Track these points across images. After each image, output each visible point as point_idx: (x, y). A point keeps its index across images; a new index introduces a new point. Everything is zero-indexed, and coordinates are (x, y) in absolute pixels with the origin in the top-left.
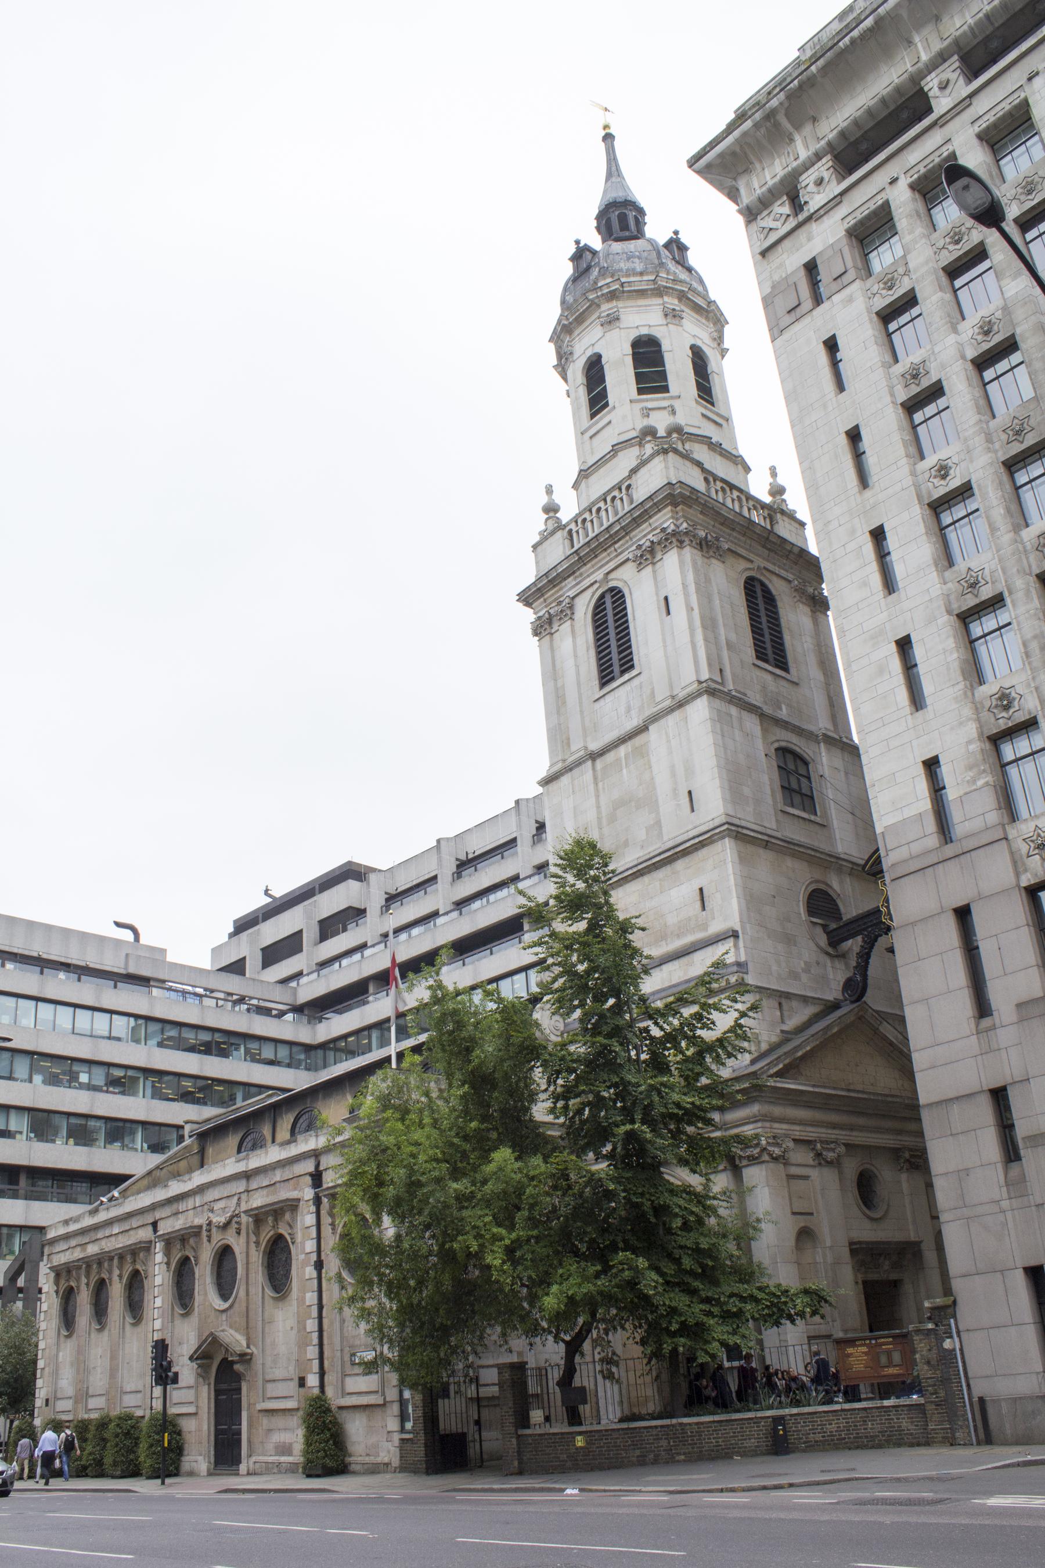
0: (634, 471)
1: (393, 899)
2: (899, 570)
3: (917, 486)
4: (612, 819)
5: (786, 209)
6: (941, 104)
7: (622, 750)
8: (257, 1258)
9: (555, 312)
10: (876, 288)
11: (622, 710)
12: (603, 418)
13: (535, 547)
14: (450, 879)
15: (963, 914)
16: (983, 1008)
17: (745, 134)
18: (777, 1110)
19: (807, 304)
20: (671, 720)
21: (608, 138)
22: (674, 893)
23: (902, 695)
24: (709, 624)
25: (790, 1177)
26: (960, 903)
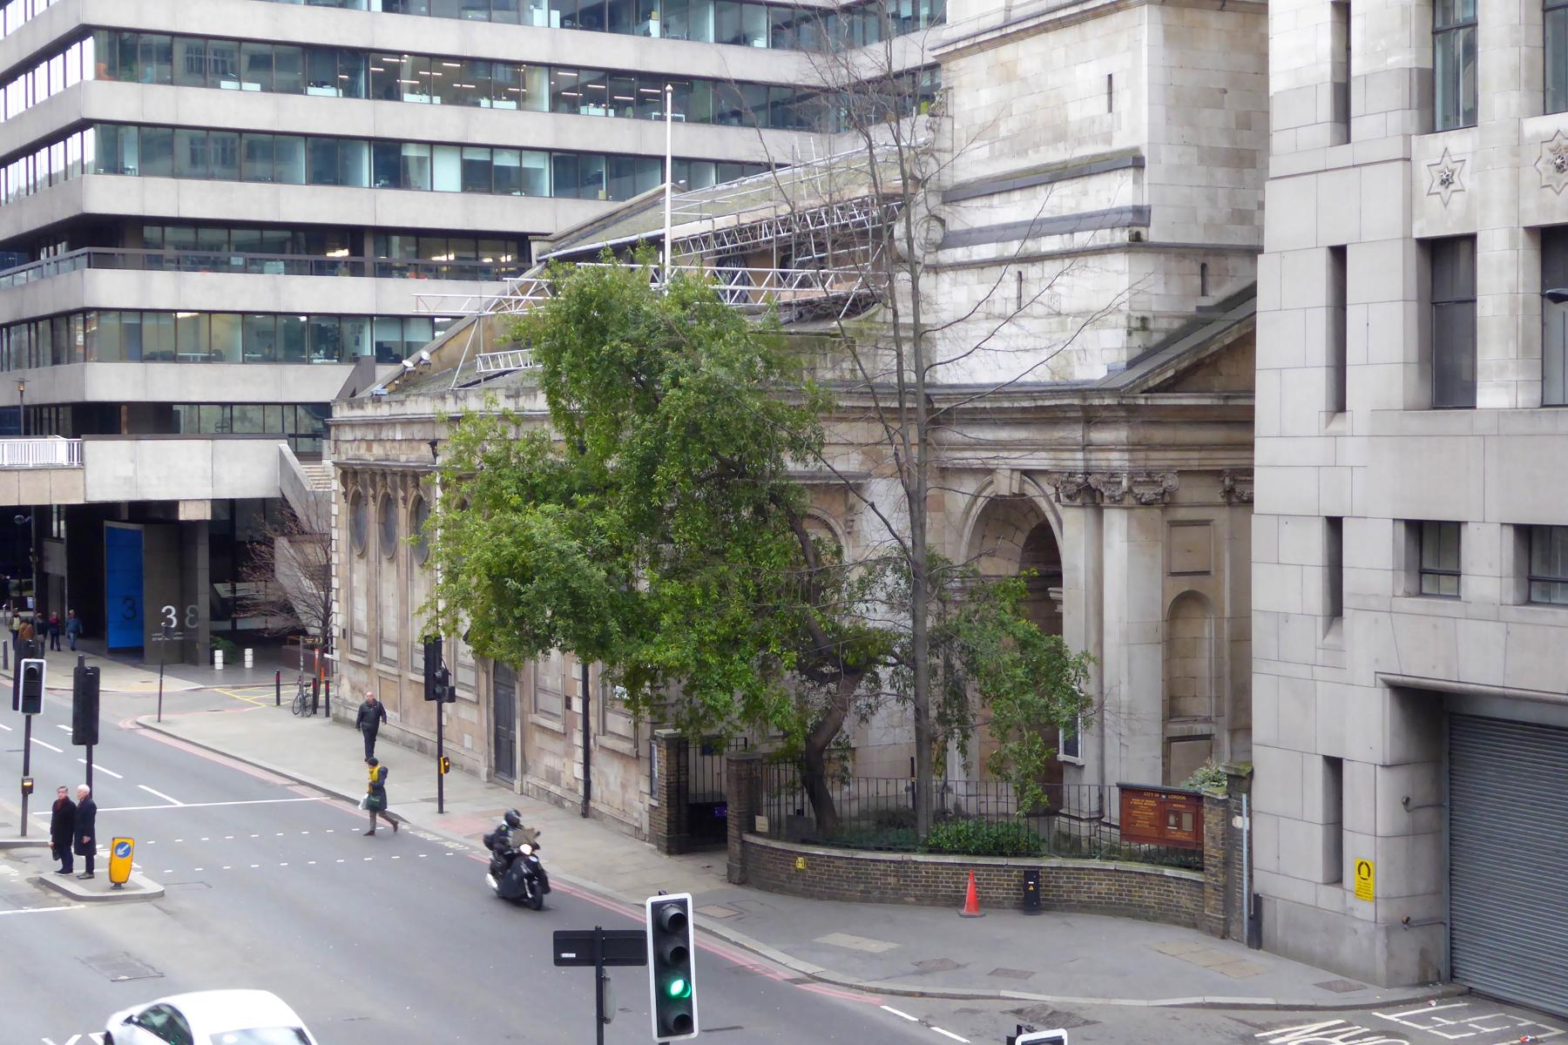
18: (1160, 435)
25: (1175, 524)
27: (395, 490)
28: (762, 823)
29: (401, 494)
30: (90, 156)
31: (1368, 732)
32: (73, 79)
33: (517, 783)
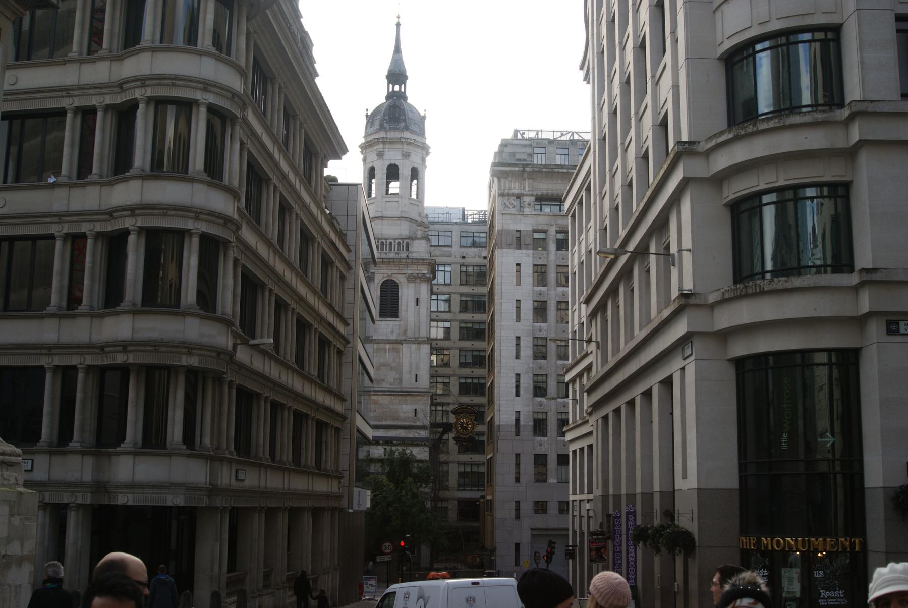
2: (522, 353)
7: (388, 346)
11: (390, 330)
16: (518, 480)
20: (414, 346)
22: (404, 406)
31: (525, 538)
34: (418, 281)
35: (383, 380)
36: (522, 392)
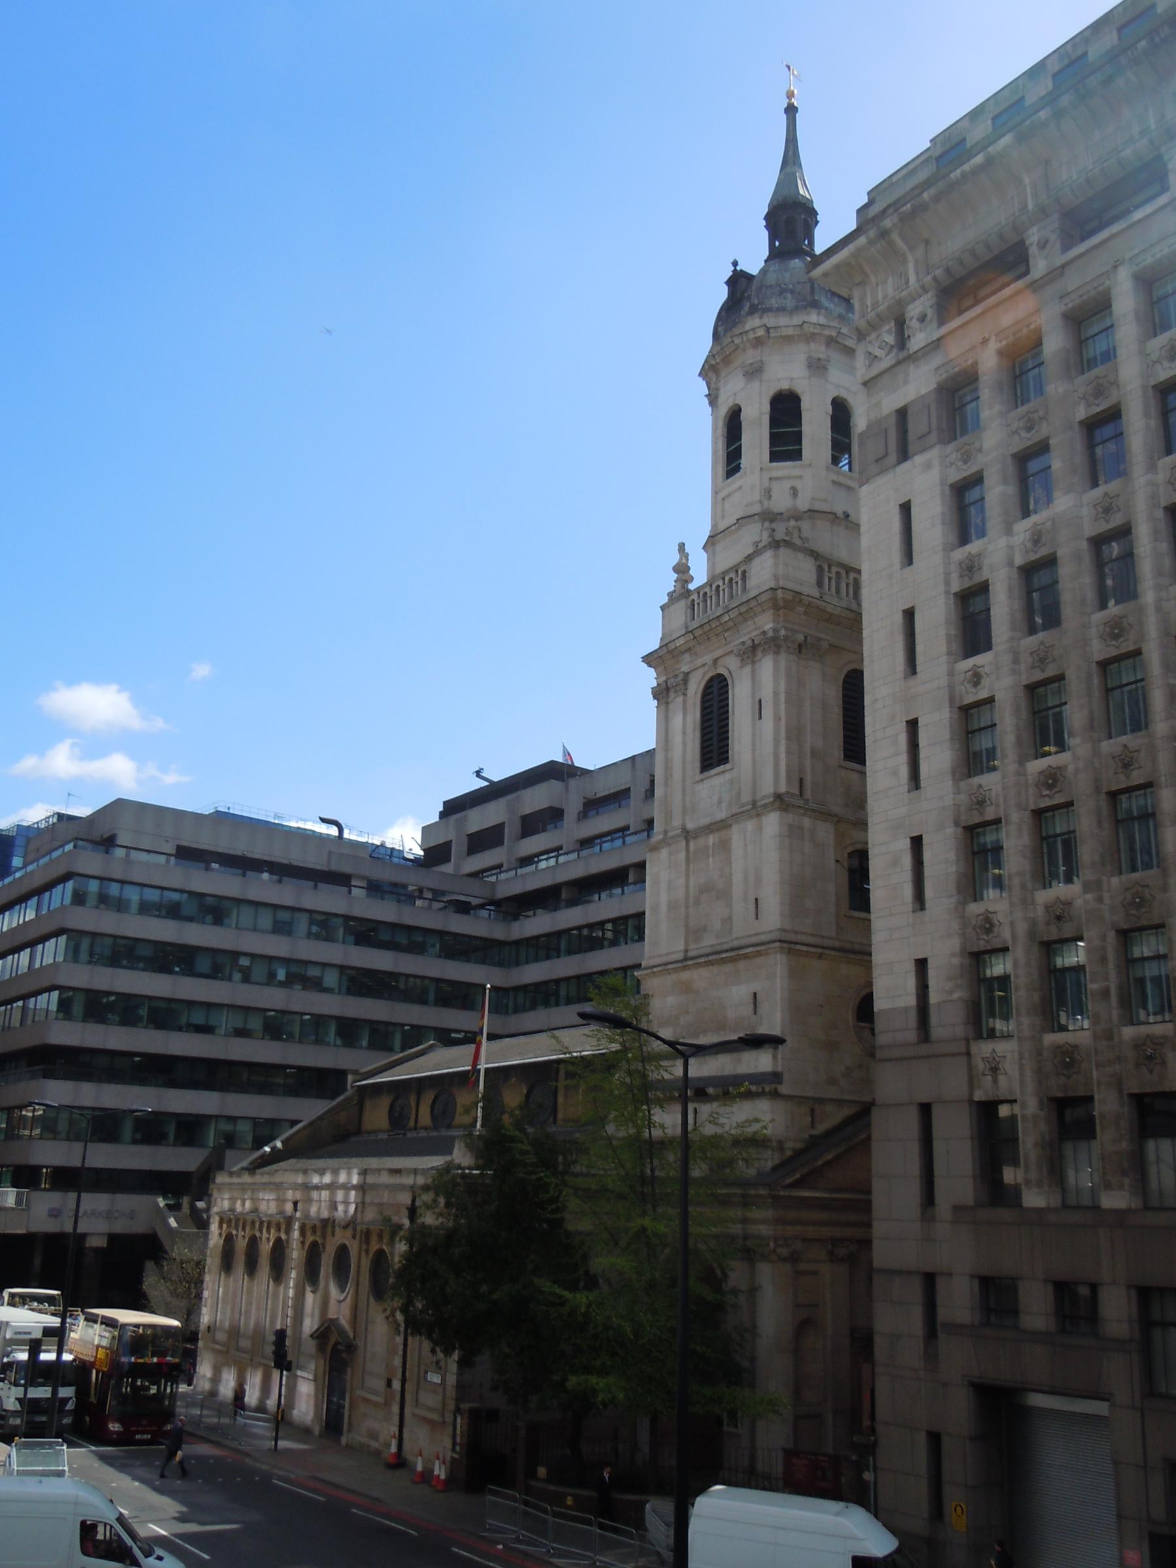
0: (749, 558)
1: (592, 806)
3: (951, 687)
4: (697, 901)
5: (890, 339)
6: (1039, 266)
8: (366, 1264)
9: (705, 343)
10: (954, 456)
12: (736, 481)
13: (663, 608)
14: (643, 796)
15: (926, 1109)
17: (859, 250)
19: (893, 457)
21: (791, 110)
22: (734, 990)
23: (908, 891)
24: (795, 734)
26: (925, 1099)
27: (261, 1231)
28: (542, 1471)
29: (265, 1235)
30: (54, 1007)
32: (48, 960)
33: (344, 1440)
34: (759, 654)
35: (705, 929)
36: (929, 893)
